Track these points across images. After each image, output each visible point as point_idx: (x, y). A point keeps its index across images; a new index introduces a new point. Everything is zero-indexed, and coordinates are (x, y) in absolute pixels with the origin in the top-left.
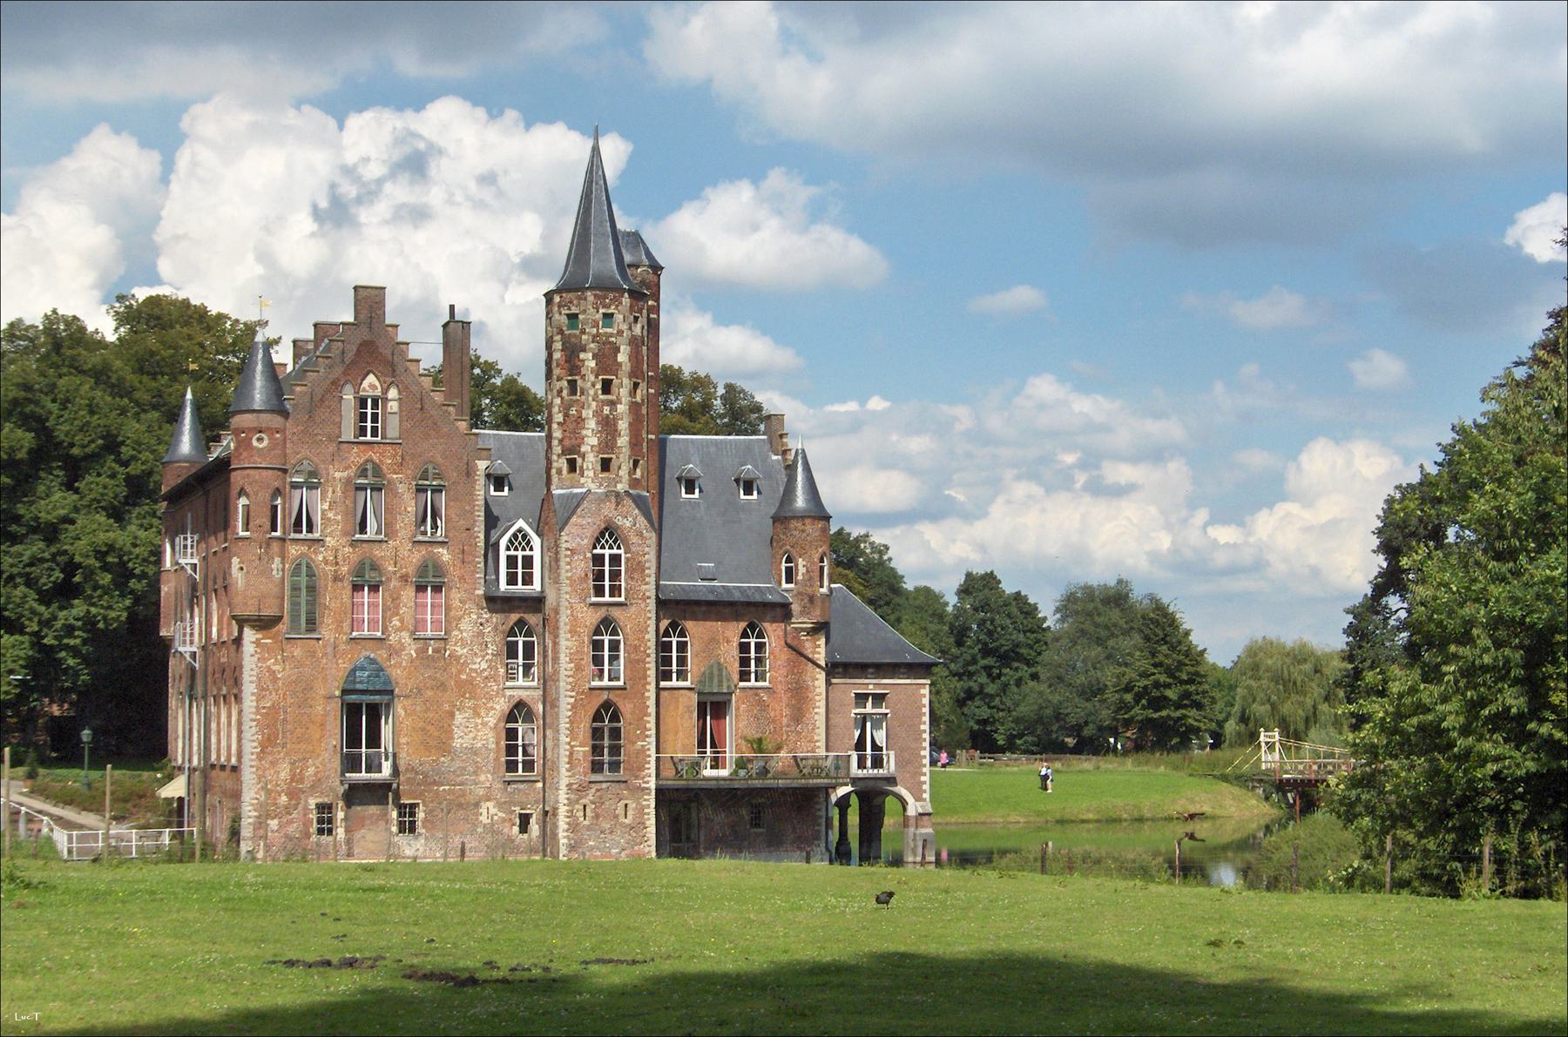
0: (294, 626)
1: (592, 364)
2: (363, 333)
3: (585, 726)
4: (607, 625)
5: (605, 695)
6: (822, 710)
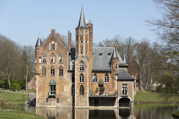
0: (43, 75)
1: (79, 39)
2: (52, 36)
3: (79, 88)
4: (82, 74)
5: (81, 84)
6: (117, 86)
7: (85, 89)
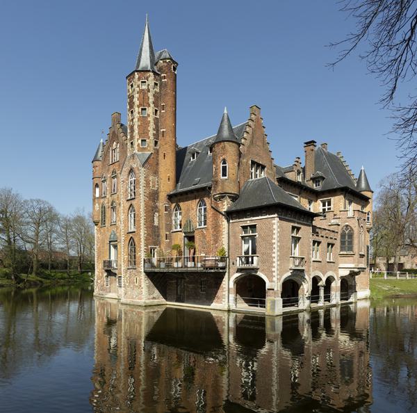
7: (137, 249)
